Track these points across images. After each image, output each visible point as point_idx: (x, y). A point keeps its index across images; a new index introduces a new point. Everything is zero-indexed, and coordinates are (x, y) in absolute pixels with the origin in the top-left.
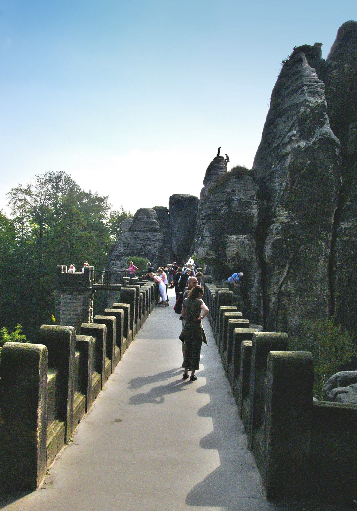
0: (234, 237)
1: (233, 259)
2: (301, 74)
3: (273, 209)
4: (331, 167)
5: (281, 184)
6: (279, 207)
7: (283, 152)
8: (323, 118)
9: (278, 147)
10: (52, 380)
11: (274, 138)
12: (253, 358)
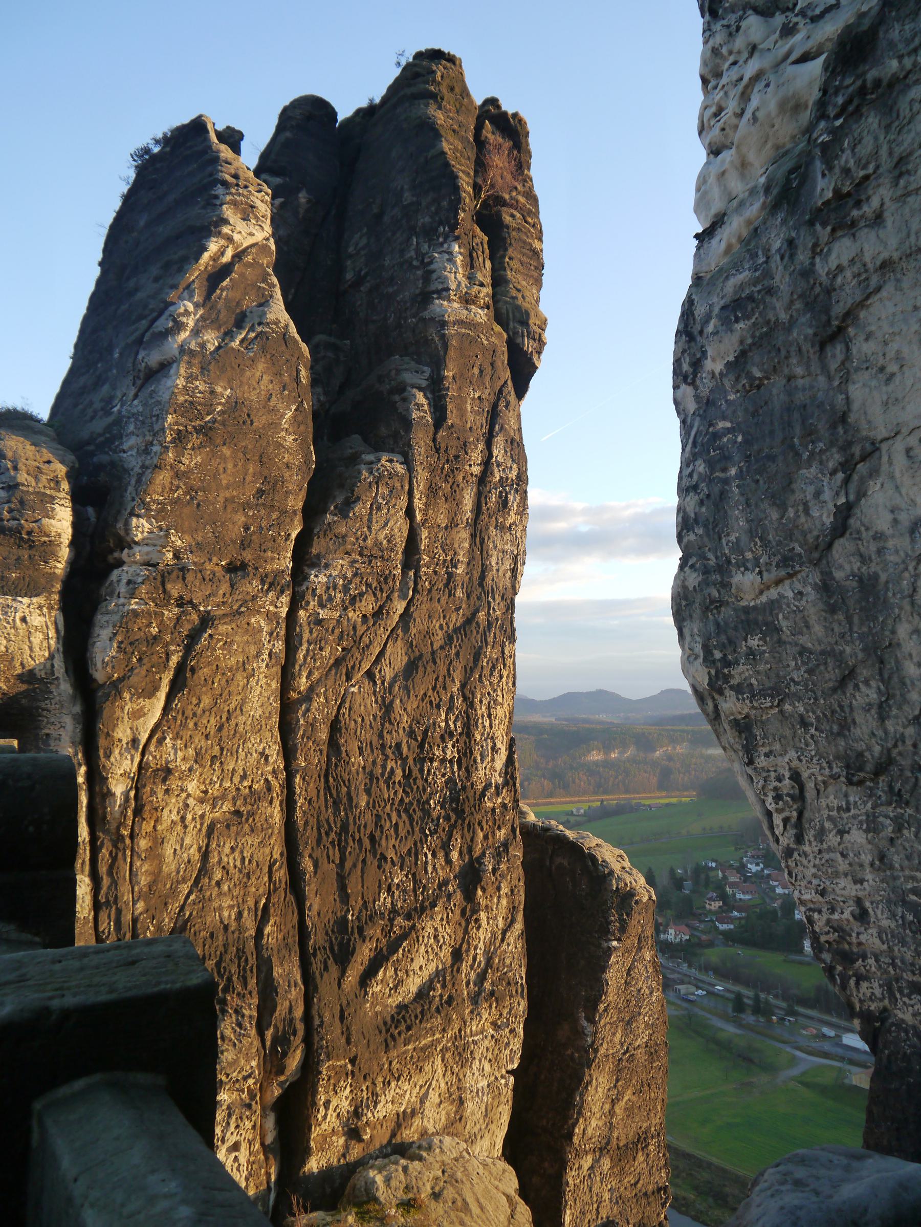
2: (207, 157)
3: (120, 525)
4: (289, 414)
6: (138, 516)
7: (153, 358)
8: (264, 280)
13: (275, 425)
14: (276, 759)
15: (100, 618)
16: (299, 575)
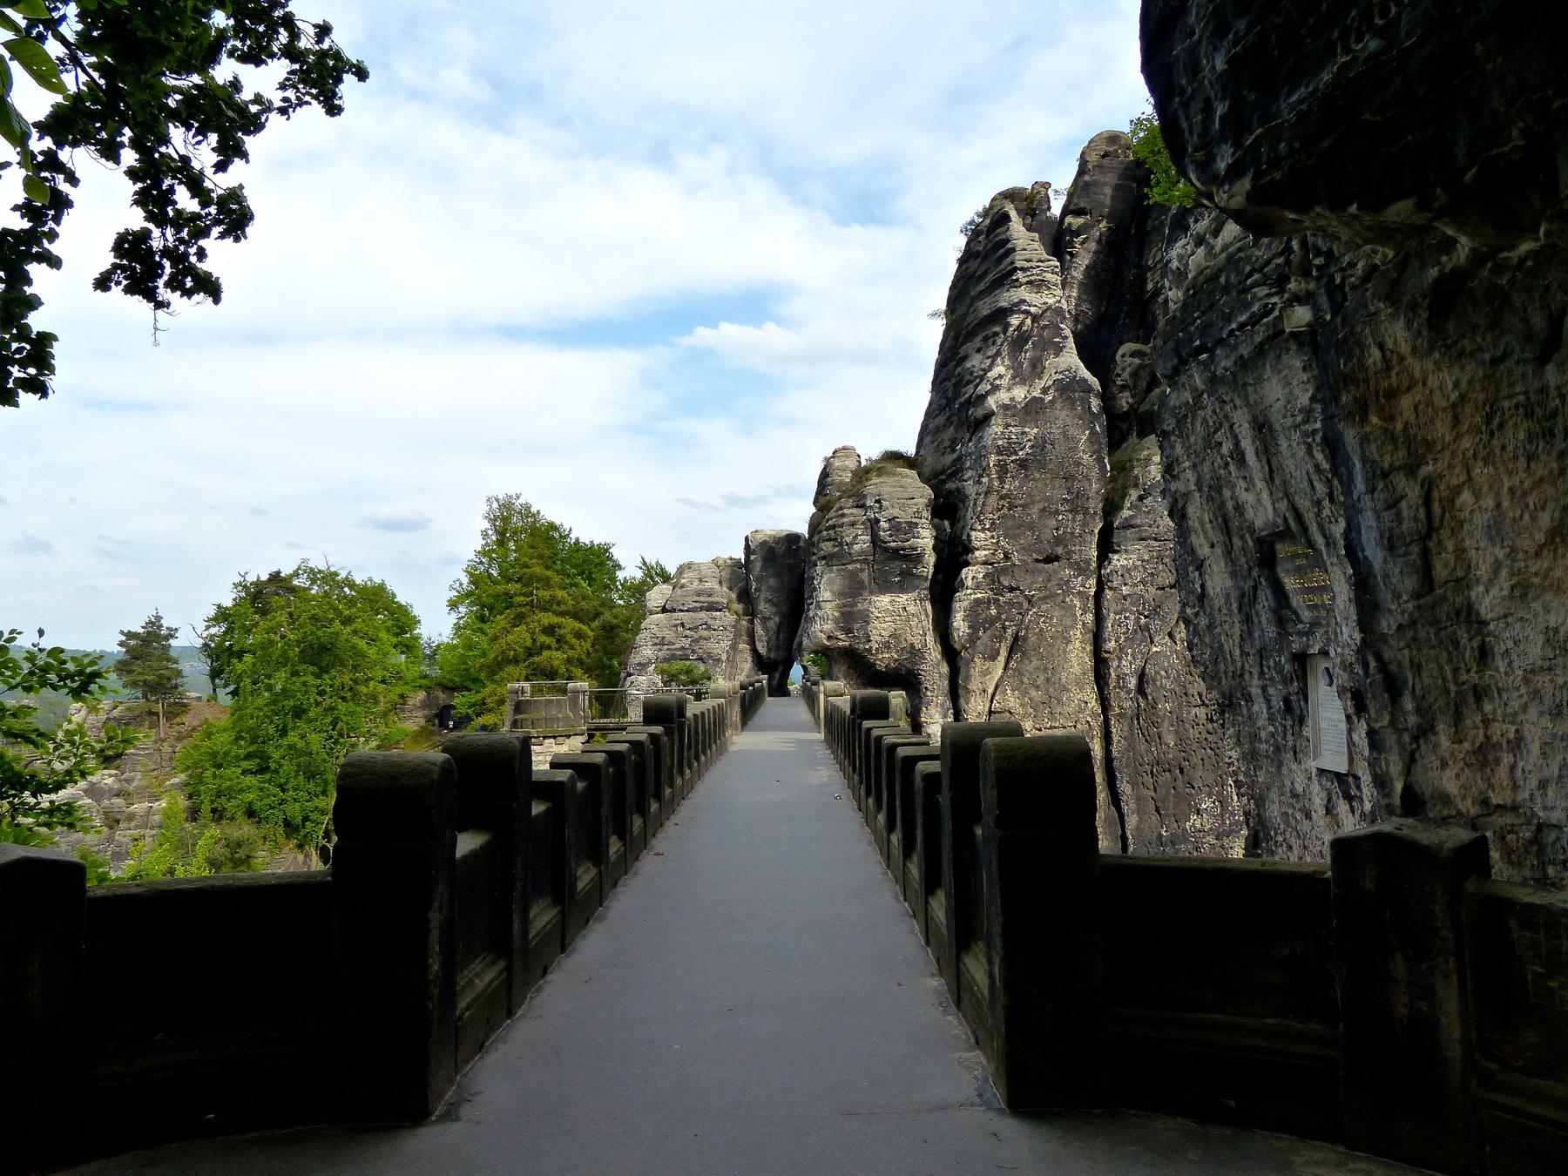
0: (884, 600)
1: (887, 645)
5: (979, 482)
7: (980, 413)
8: (1059, 335)
9: (968, 402)
10: (473, 856)
11: (960, 383)
12: (944, 799)
13: (1075, 449)
14: (1094, 704)
15: (957, 605)
16: (1103, 558)
